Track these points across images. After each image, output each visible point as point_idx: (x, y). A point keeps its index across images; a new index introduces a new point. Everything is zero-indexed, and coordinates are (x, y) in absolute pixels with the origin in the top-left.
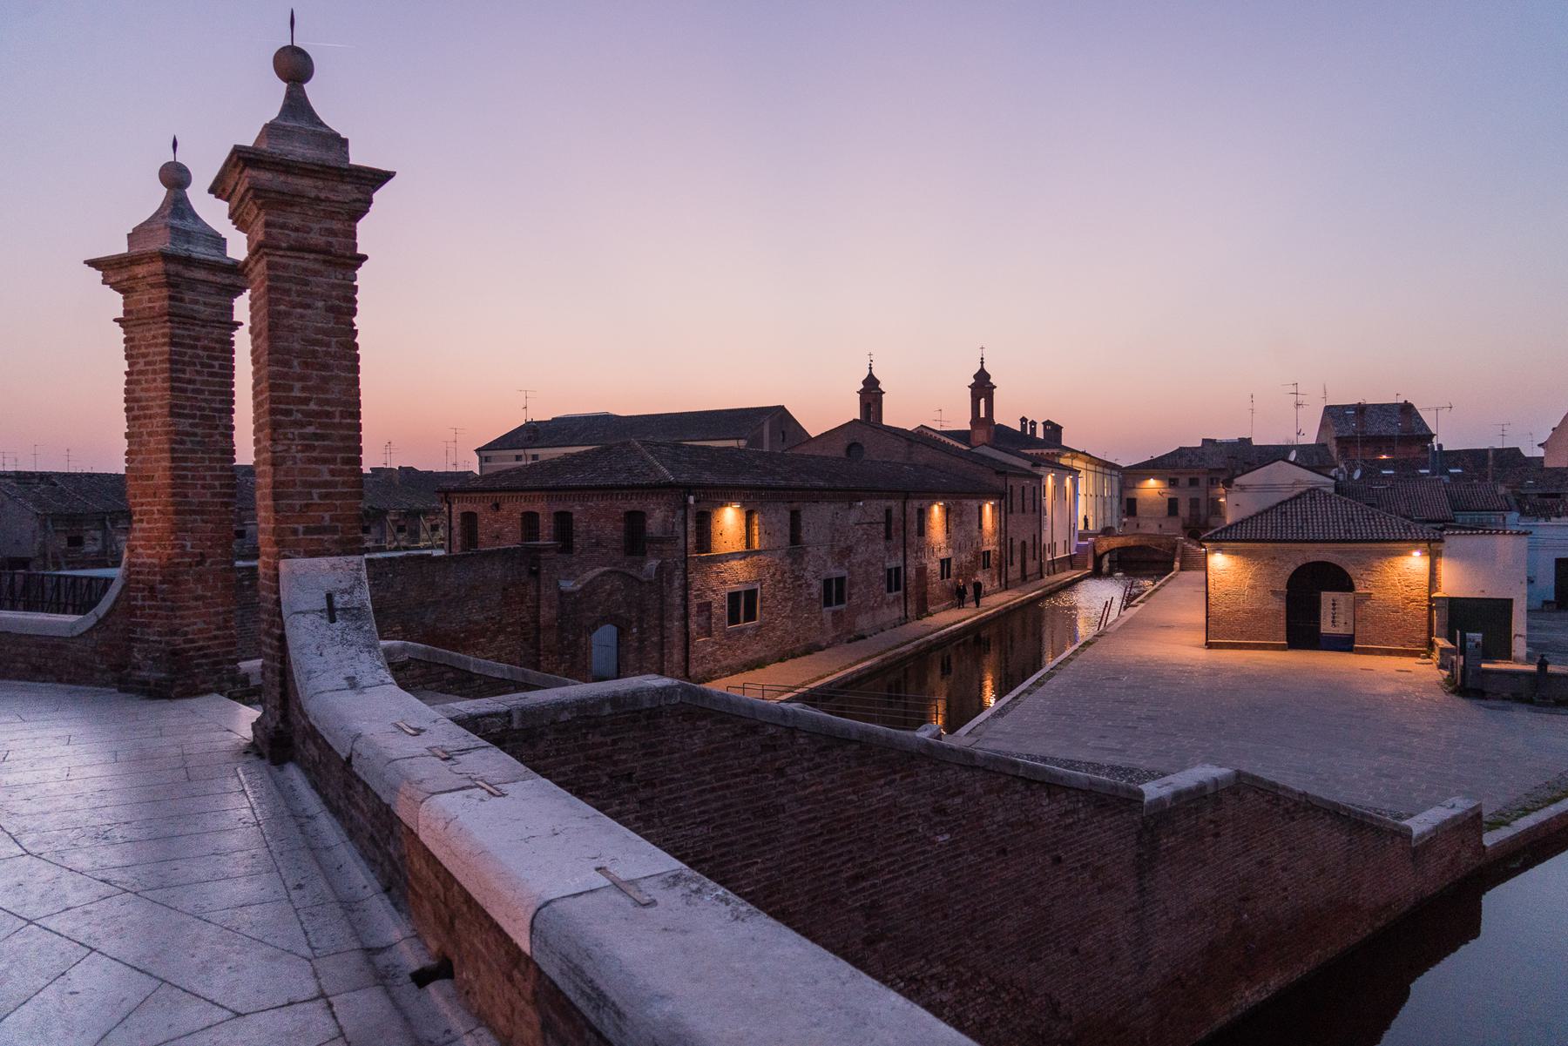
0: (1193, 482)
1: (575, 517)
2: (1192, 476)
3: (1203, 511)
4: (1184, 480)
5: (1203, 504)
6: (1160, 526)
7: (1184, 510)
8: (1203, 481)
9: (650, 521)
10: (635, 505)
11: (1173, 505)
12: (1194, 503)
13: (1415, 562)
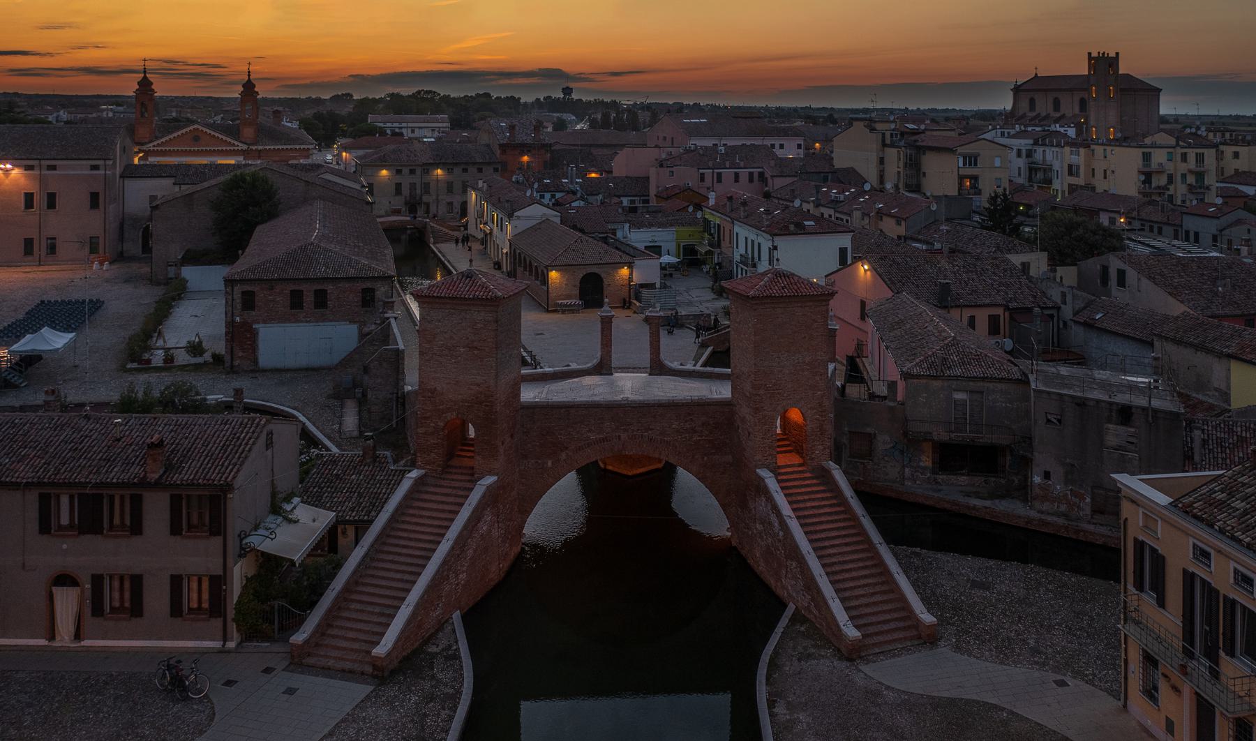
0: (412, 172)
1: (328, 292)
2: (411, 168)
3: (418, 192)
4: (406, 171)
5: (418, 187)
6: (390, 203)
7: (406, 191)
8: (418, 171)
9: (378, 292)
10: (368, 285)
11: (398, 186)
12: (413, 186)
13: (625, 271)
